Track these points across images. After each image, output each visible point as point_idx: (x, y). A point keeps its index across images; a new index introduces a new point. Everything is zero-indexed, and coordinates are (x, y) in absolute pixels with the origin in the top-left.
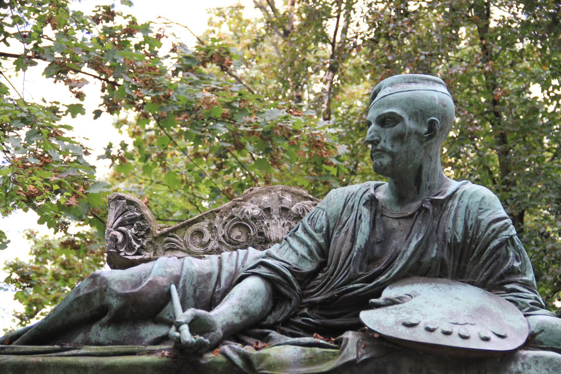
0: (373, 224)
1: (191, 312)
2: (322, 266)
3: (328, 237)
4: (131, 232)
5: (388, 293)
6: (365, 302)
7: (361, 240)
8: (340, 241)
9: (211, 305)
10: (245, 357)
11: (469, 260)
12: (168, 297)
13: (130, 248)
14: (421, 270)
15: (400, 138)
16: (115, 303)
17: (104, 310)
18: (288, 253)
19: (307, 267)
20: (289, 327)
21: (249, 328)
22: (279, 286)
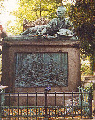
0: (58, 23)
1: (40, 32)
2: (52, 27)
3: (53, 24)
4: (26, 23)
5: (59, 30)
6: (58, 31)
7: (56, 25)
8: (54, 25)
9: (41, 31)
10: (46, 37)
11: (67, 27)
12: (37, 30)
13: (26, 25)
14: (62, 28)
15: (60, 13)
16: (31, 31)
17: (30, 32)
18: (49, 26)
19: (50, 27)
20: (50, 34)
21: (45, 34)
22: (48, 30)
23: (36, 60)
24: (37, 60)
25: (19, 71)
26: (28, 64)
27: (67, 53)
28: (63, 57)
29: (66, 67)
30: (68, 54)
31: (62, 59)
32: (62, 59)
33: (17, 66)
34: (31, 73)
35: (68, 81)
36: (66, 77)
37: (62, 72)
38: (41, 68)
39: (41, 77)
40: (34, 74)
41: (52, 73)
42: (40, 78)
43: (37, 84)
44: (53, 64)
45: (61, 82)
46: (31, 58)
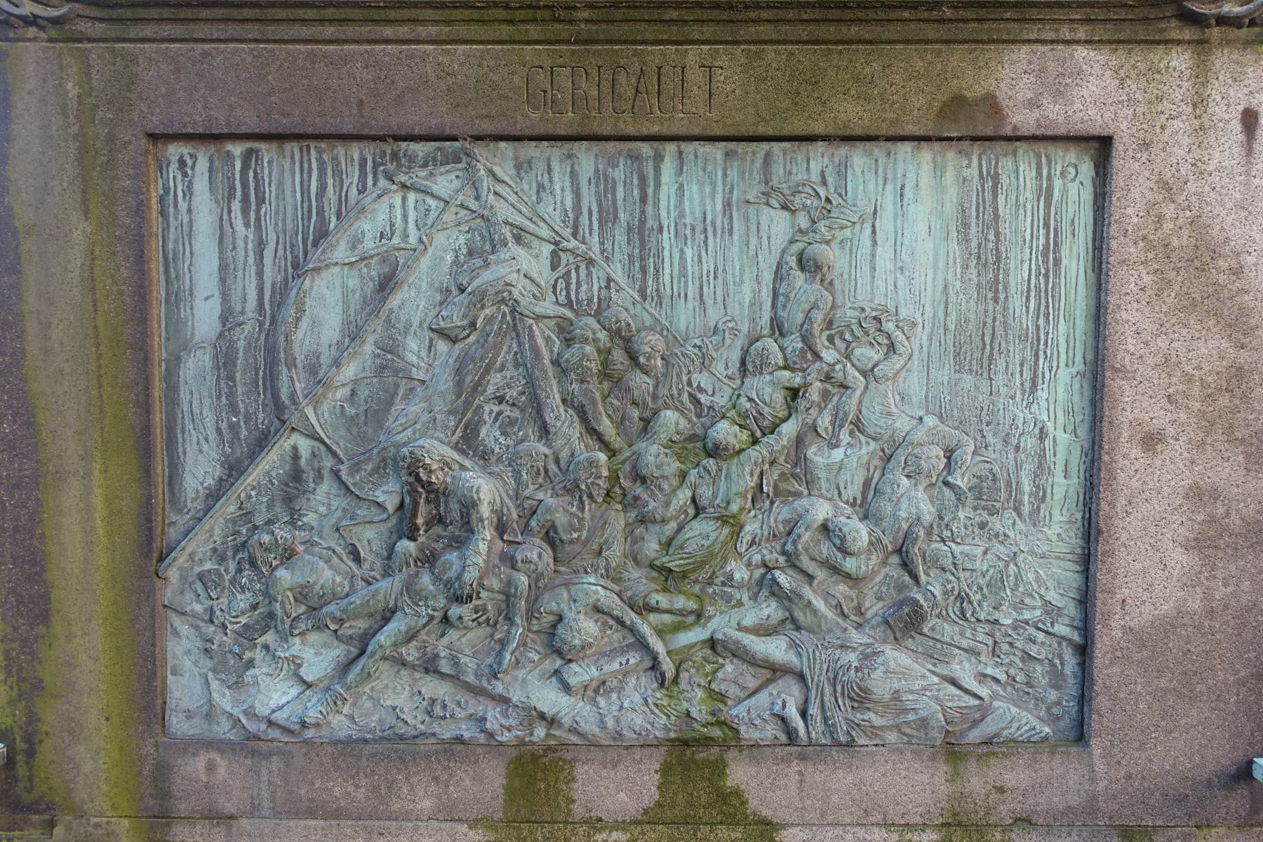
23: (524, 269)
24: (544, 275)
25: (234, 470)
26: (390, 348)
27: (1101, 147)
28: (1020, 227)
29: (1057, 403)
30: (1124, 163)
31: (988, 264)
32: (994, 288)
33: (196, 367)
34: (430, 512)
35: (1084, 651)
36: (1053, 579)
37: (988, 494)
38: (621, 422)
39: (613, 576)
40: (501, 528)
41: (821, 510)
42: (594, 588)
43: (548, 698)
44: (829, 355)
45: (964, 671)
46: (449, 242)
